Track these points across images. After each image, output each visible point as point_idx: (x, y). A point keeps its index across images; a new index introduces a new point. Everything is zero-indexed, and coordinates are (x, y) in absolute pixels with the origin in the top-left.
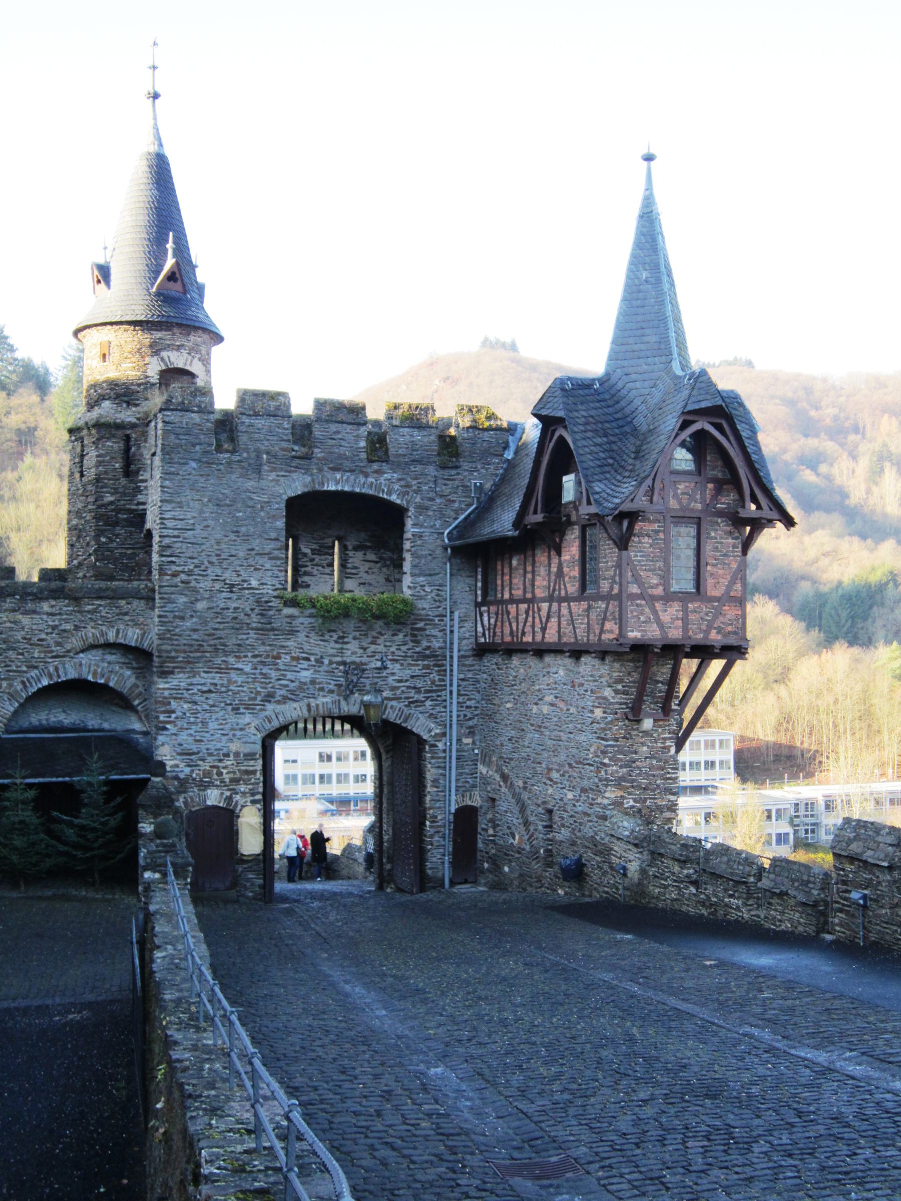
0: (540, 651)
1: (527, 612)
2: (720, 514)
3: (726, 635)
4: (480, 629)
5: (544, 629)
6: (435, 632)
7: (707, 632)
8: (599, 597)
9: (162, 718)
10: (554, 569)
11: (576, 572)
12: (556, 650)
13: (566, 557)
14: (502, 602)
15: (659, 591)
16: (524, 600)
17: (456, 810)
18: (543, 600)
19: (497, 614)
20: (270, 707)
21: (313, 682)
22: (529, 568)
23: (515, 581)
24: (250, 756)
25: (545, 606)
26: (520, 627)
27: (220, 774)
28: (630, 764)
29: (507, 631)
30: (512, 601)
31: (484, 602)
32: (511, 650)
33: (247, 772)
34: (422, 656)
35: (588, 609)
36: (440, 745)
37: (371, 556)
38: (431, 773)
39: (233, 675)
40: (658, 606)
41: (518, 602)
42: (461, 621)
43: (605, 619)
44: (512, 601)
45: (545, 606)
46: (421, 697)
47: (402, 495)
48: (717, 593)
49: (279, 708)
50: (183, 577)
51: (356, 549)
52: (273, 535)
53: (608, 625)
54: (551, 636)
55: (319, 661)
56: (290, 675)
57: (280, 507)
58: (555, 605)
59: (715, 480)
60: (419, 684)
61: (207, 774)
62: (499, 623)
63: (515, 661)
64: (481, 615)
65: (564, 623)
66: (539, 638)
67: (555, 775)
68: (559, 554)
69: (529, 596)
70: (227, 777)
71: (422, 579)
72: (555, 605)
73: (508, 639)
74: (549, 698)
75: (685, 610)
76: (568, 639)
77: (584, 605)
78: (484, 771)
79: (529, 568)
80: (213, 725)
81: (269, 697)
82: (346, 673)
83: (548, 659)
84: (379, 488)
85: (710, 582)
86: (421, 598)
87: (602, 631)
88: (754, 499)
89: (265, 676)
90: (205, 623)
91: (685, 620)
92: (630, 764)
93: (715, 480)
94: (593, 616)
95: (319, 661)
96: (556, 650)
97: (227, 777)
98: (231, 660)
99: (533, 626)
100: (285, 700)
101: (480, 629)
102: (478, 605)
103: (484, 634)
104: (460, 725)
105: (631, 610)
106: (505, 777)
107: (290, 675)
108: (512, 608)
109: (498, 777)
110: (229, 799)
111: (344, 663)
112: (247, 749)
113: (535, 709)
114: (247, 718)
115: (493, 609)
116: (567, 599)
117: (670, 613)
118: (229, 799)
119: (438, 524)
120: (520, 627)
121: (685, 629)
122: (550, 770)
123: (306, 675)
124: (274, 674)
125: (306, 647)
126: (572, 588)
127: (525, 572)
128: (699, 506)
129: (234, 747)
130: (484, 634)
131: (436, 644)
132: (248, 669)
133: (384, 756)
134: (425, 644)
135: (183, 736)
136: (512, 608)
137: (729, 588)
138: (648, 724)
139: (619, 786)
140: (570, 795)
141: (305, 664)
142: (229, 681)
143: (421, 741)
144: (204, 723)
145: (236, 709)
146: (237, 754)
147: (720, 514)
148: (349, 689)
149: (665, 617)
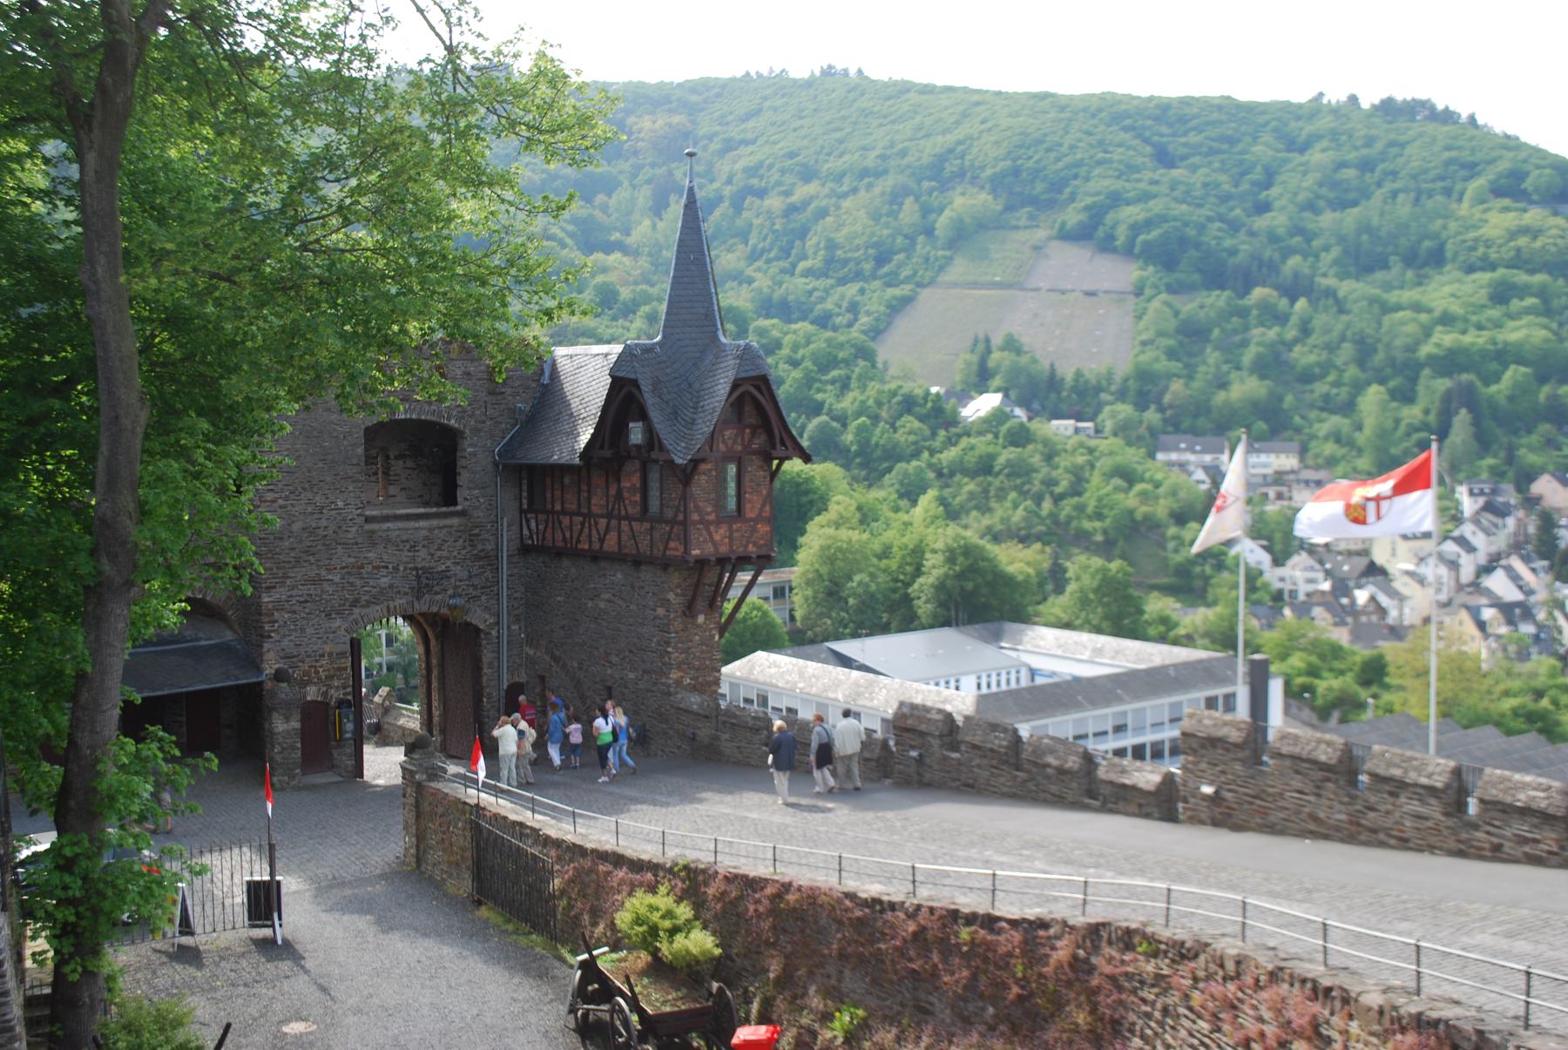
0: (595, 557)
1: (583, 524)
2: (755, 453)
3: (760, 547)
4: (526, 532)
5: (602, 541)
6: (487, 536)
7: (746, 546)
8: (661, 519)
9: (267, 627)
10: (613, 492)
11: (638, 498)
12: (618, 558)
13: (626, 484)
14: (553, 512)
15: (712, 517)
16: (579, 514)
17: (509, 687)
18: (602, 516)
19: (547, 522)
20: (356, 611)
21: (391, 586)
22: (584, 488)
23: (568, 496)
24: (342, 654)
25: (603, 522)
26: (575, 535)
27: (317, 672)
28: (687, 651)
29: (559, 536)
30: (564, 512)
31: (530, 510)
32: (559, 554)
33: (339, 669)
34: (478, 558)
35: (652, 528)
36: (494, 633)
37: (410, 464)
38: (487, 656)
39: (325, 585)
40: (712, 528)
41: (572, 514)
42: (509, 525)
43: (669, 538)
44: (564, 512)
45: (603, 522)
46: (478, 593)
47: (459, 419)
48: (752, 515)
49: (364, 611)
50: (281, 502)
51: (397, 458)
52: (355, 461)
53: (672, 544)
54: (611, 544)
55: (396, 569)
56: (372, 582)
57: (359, 435)
58: (614, 522)
59: (750, 426)
60: (476, 581)
61: (306, 673)
62: (549, 531)
63: (566, 562)
64: (528, 521)
65: (624, 538)
66: (596, 546)
67: (614, 659)
68: (618, 480)
69: (585, 511)
70: (323, 675)
71: (476, 492)
72: (614, 522)
73: (561, 544)
74: (607, 596)
75: (730, 529)
76: (629, 548)
77: (647, 525)
78: (531, 652)
79: (584, 488)
80: (309, 631)
81: (355, 604)
82: (418, 577)
83: (603, 564)
84: (440, 413)
85: (748, 506)
86: (477, 508)
87: (666, 548)
88: (783, 443)
89: (351, 584)
90: (301, 542)
91: (731, 538)
92: (687, 651)
93: (750, 426)
94: (657, 535)
95: (396, 569)
96: (618, 558)
97: (323, 675)
98: (323, 573)
99: (590, 536)
100: (368, 604)
101: (526, 532)
102: (521, 511)
103: (531, 537)
104: (509, 614)
105: (693, 535)
106: (555, 659)
107: (372, 582)
108: (566, 520)
109: (547, 658)
110: (325, 694)
111: (416, 569)
112: (339, 648)
113: (590, 604)
114: (338, 622)
115: (542, 517)
116: (629, 518)
117: (720, 534)
118: (325, 694)
119: (489, 443)
120: (575, 535)
121: (731, 545)
122: (608, 654)
123: (385, 581)
124: (358, 583)
125: (385, 557)
126: (633, 510)
127: (579, 491)
128: (739, 448)
129: (328, 648)
130: (531, 537)
131: (489, 547)
132: (337, 579)
133: (433, 642)
134: (480, 547)
135: (285, 643)
136: (566, 520)
137: (761, 510)
138: (701, 619)
139: (679, 668)
140: (631, 676)
141: (384, 572)
142: (323, 591)
143: (477, 630)
144: (303, 630)
145: (328, 615)
146: (330, 654)
147: (755, 453)
148: (418, 593)
149: (717, 537)
